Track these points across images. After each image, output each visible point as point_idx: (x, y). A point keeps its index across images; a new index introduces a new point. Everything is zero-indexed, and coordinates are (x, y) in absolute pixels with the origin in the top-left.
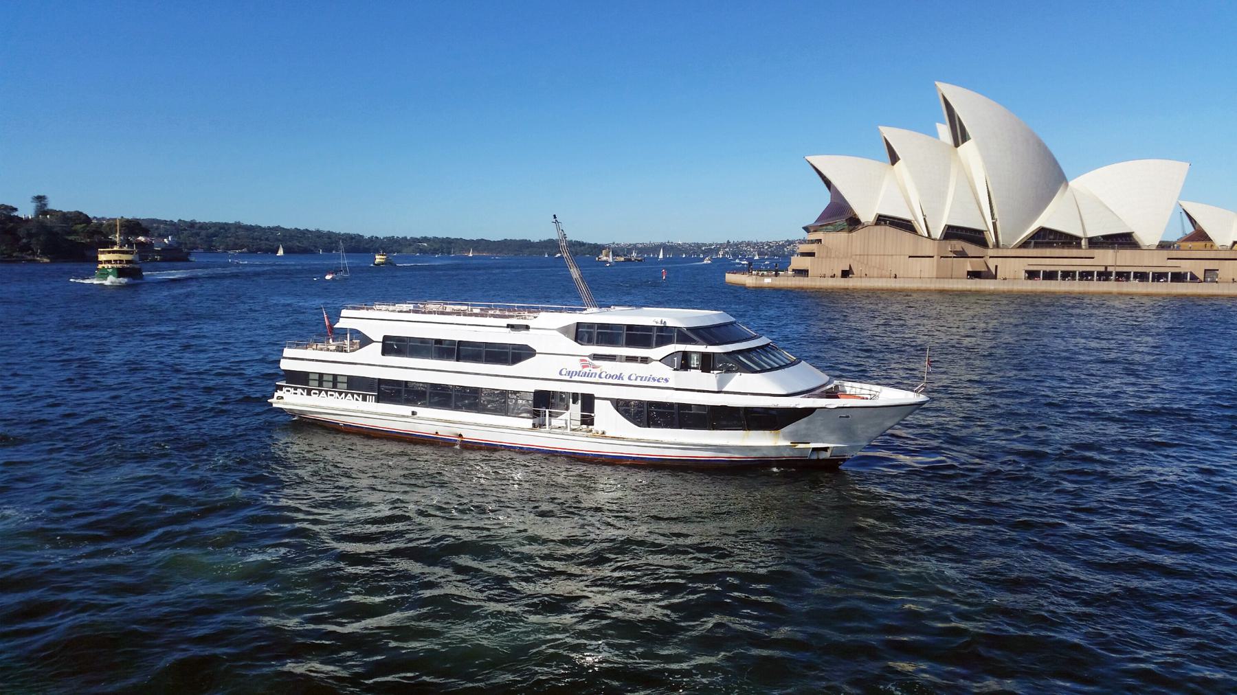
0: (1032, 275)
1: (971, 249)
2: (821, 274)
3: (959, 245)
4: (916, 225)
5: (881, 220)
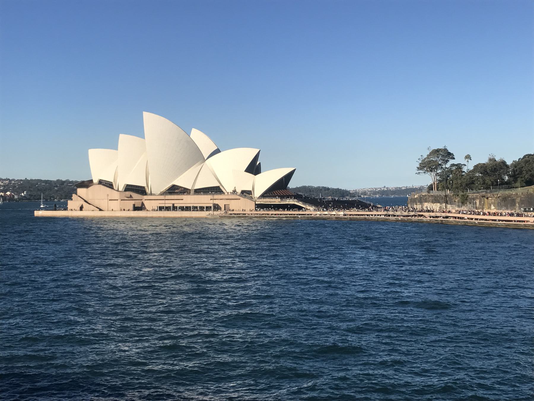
0: (161, 208)
1: (135, 196)
2: (73, 209)
3: (128, 193)
4: (114, 185)
5: (101, 182)
